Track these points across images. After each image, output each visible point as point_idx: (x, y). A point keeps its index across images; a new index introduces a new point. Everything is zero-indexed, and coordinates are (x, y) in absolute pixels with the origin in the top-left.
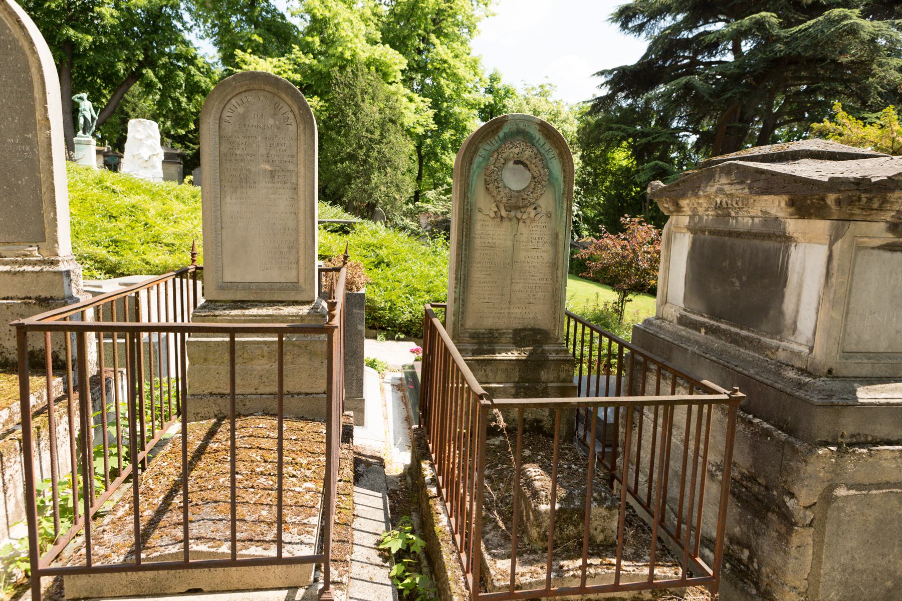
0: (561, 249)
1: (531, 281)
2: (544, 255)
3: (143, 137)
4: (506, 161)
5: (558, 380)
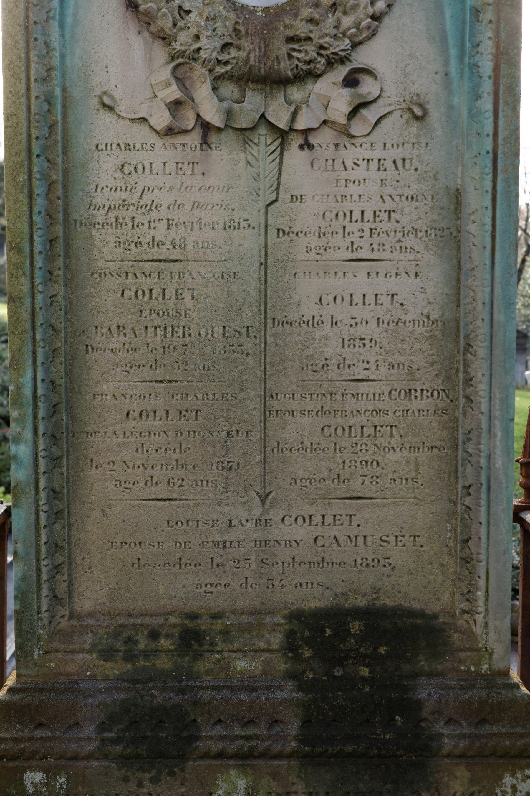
1: (351, 404)
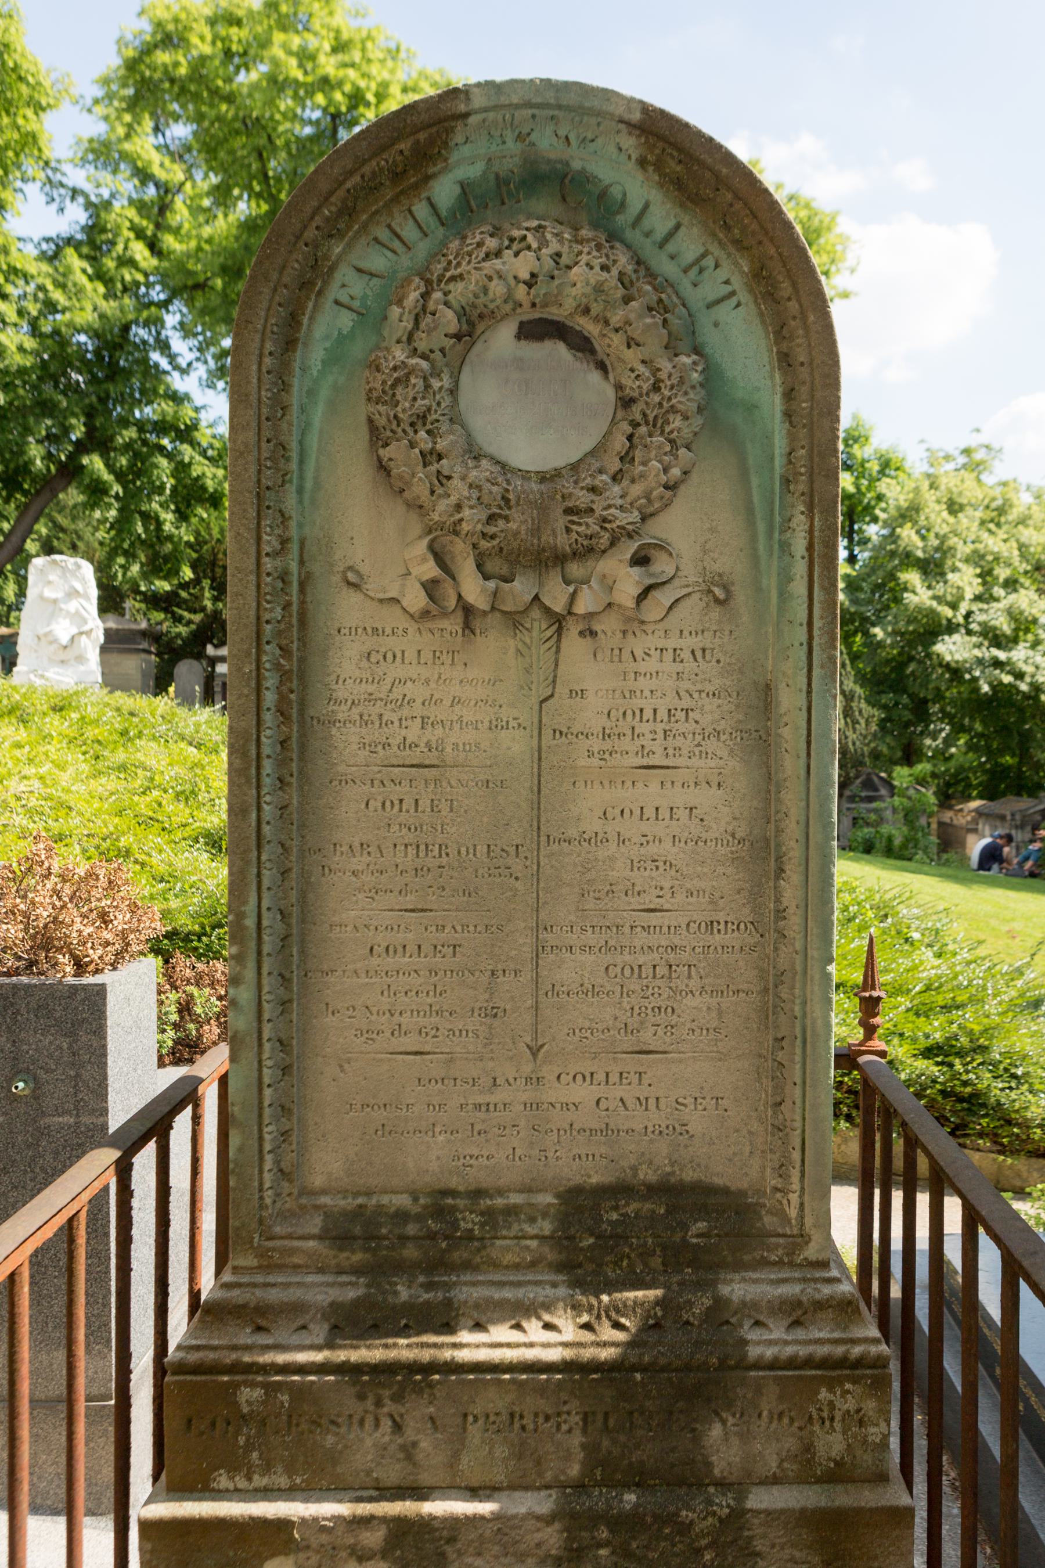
0: (791, 766)
1: (641, 939)
2: (706, 798)
3: (59, 595)
4: (471, 327)
5: (807, 1469)
